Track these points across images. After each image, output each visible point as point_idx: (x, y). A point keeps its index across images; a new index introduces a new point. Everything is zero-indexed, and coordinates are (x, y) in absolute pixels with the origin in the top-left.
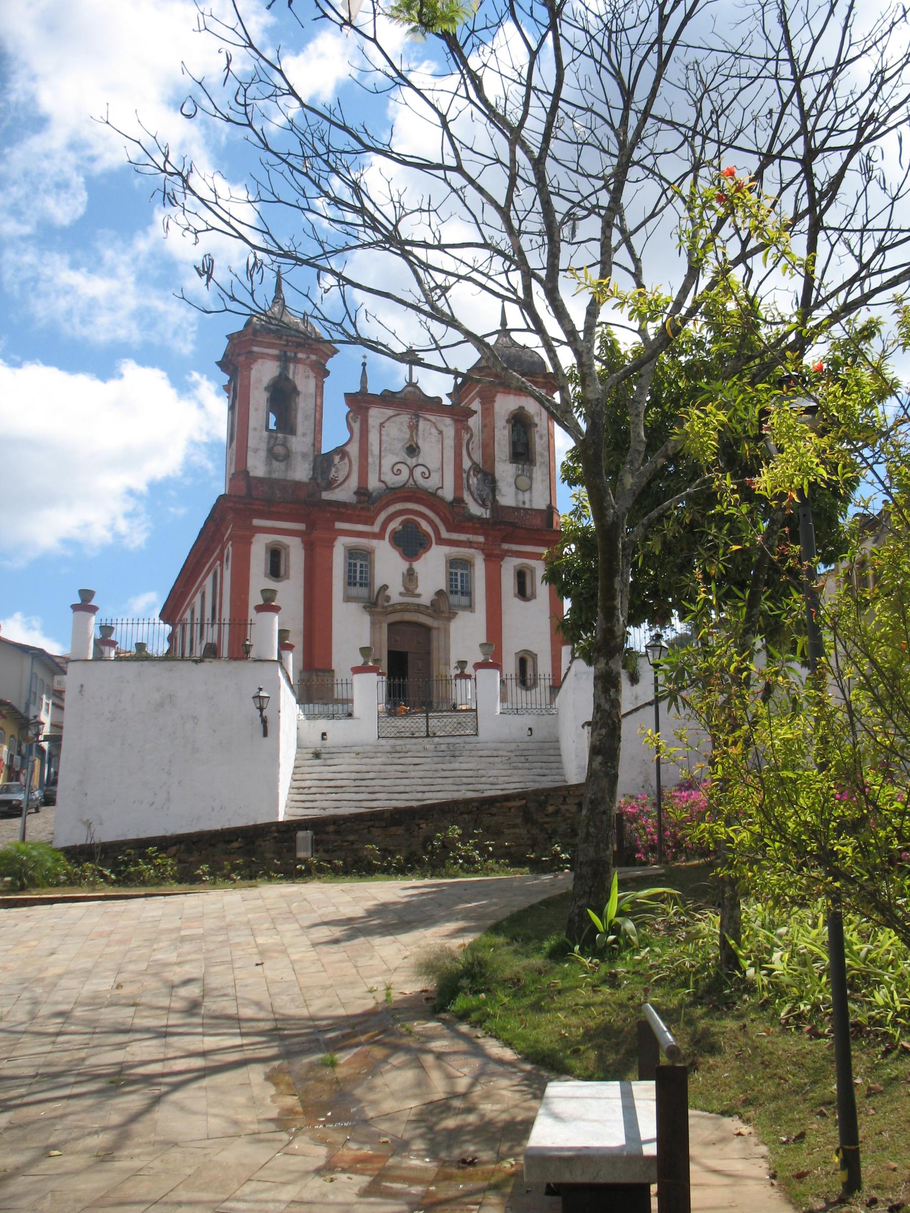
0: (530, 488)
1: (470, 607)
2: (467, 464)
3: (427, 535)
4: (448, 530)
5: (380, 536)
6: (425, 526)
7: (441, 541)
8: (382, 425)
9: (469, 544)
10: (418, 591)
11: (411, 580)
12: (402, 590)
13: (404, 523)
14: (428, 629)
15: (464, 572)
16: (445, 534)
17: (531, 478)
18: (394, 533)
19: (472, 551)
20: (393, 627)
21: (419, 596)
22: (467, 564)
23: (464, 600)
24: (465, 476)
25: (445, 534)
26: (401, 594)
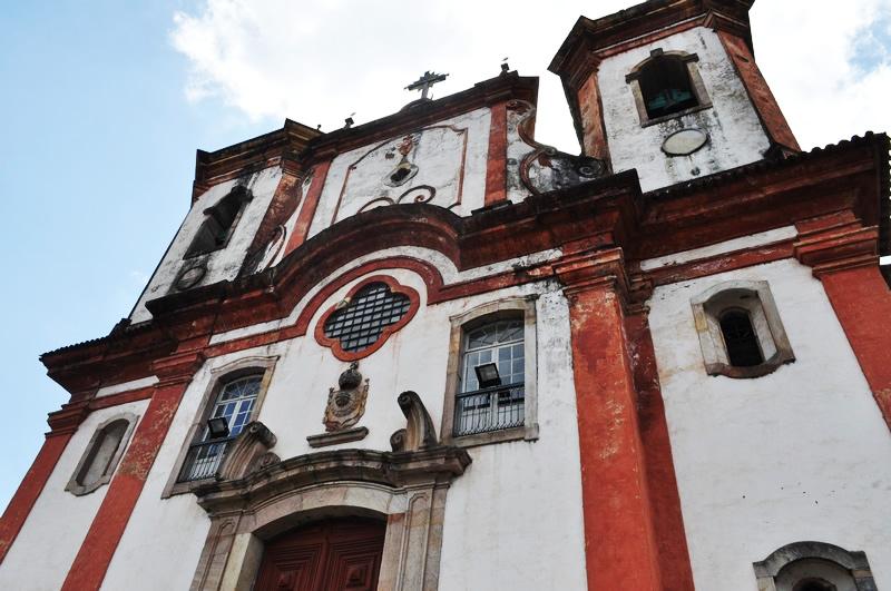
0: (707, 142)
1: (519, 433)
2: (517, 150)
3: (406, 298)
4: (462, 267)
5: (298, 330)
6: (407, 279)
7: (441, 293)
8: (352, 167)
9: (520, 276)
10: (359, 425)
11: (342, 401)
12: (321, 430)
13: (357, 294)
14: (371, 526)
15: (510, 345)
16: (451, 275)
17: (704, 127)
18: (333, 315)
19: (529, 289)
20: (272, 541)
21: (363, 432)
22: (511, 321)
23: (501, 416)
24: (513, 169)
25: (451, 275)
26: (314, 441)
